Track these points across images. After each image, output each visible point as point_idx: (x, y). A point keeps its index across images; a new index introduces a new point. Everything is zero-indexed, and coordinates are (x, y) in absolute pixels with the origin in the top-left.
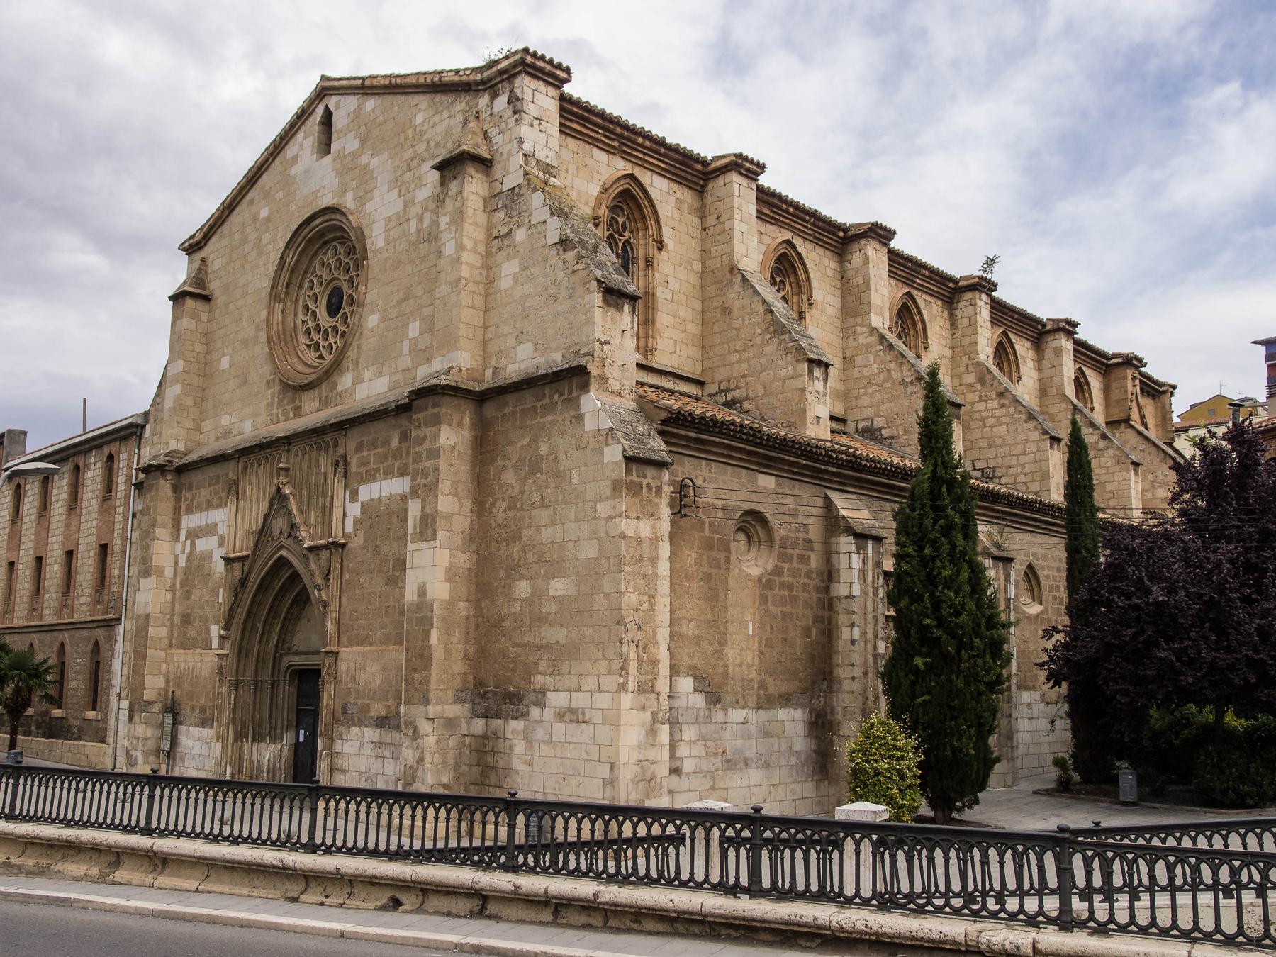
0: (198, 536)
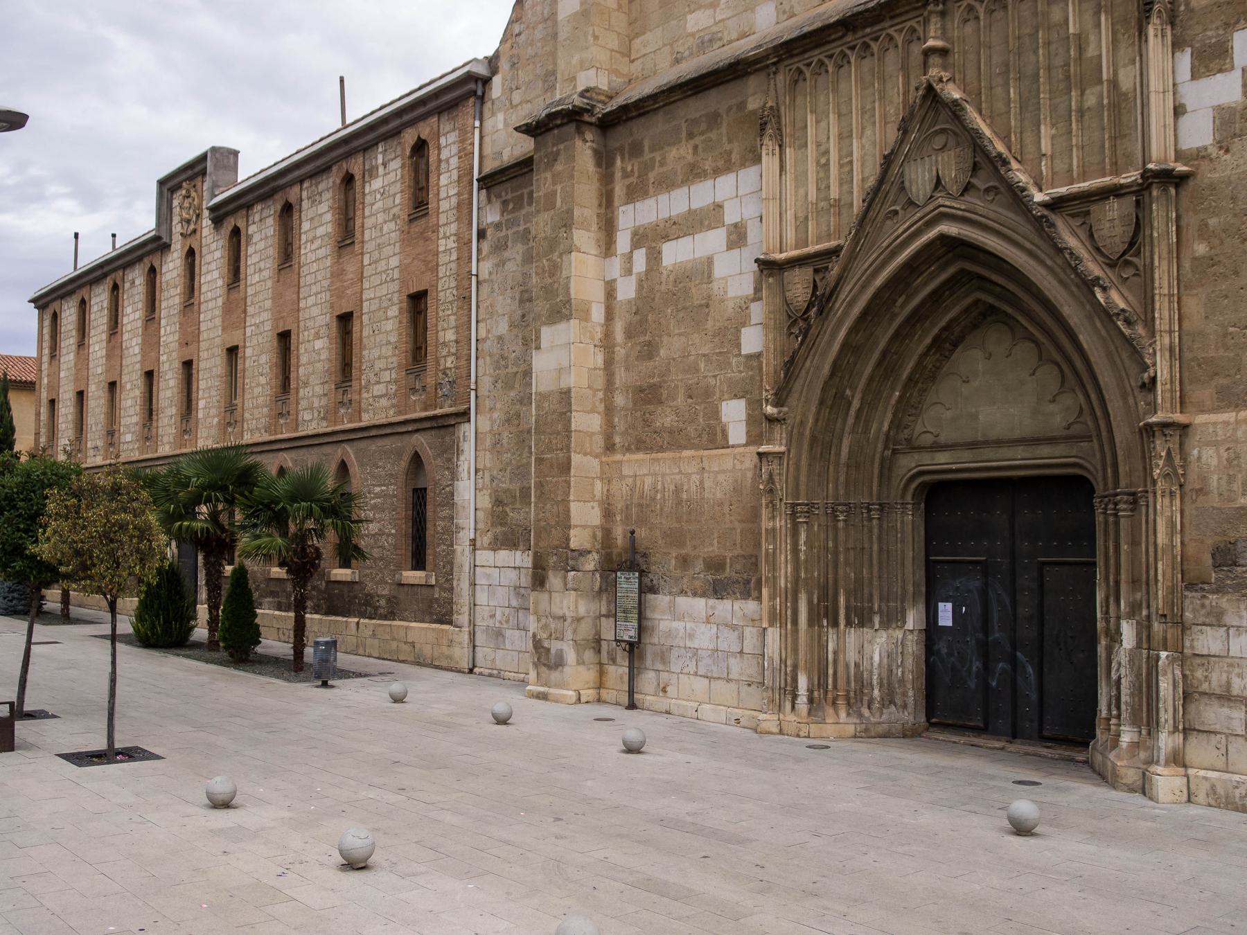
0: (666, 238)
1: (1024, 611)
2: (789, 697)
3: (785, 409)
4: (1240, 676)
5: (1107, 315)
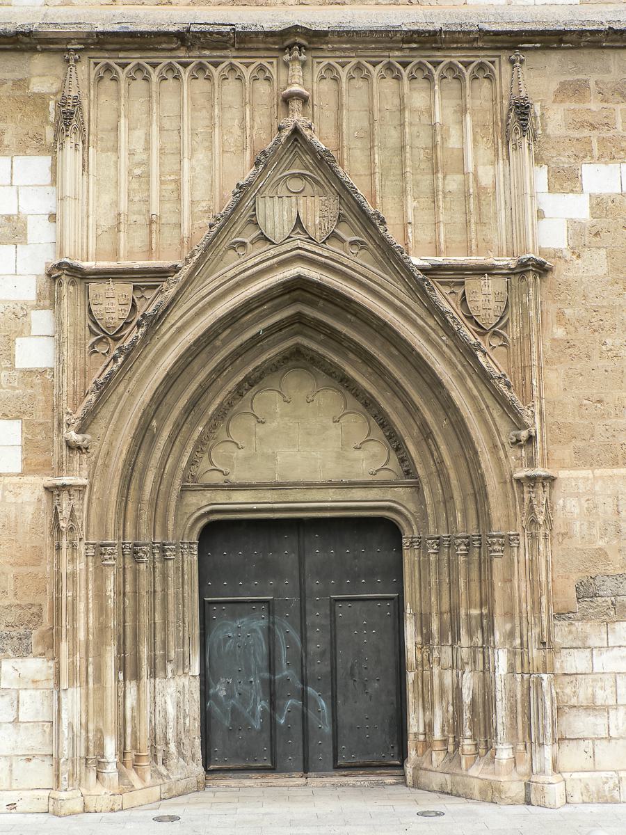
1: (315, 647)
2: (93, 767)
3: (88, 436)
4: (603, 688)
5: (485, 377)
